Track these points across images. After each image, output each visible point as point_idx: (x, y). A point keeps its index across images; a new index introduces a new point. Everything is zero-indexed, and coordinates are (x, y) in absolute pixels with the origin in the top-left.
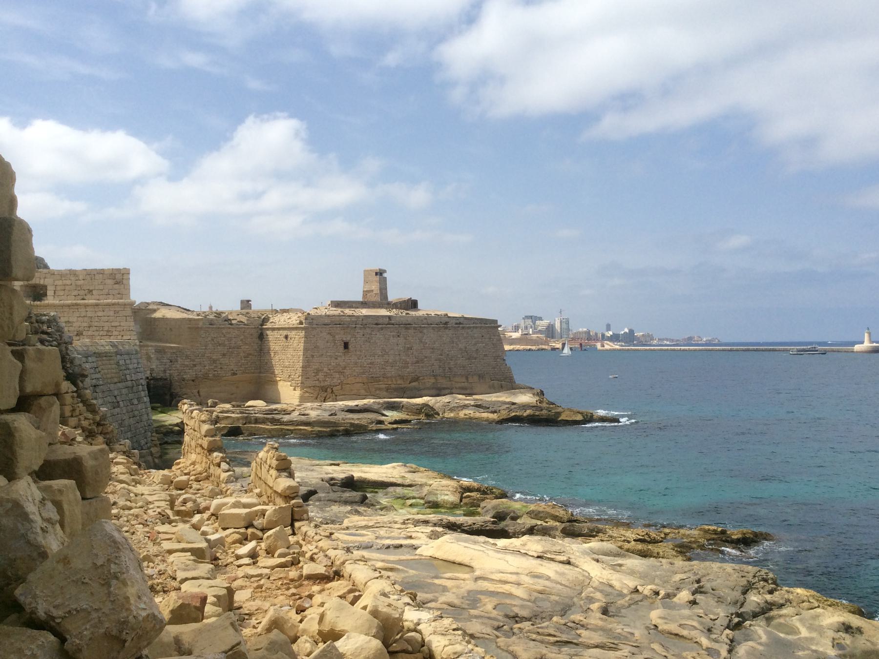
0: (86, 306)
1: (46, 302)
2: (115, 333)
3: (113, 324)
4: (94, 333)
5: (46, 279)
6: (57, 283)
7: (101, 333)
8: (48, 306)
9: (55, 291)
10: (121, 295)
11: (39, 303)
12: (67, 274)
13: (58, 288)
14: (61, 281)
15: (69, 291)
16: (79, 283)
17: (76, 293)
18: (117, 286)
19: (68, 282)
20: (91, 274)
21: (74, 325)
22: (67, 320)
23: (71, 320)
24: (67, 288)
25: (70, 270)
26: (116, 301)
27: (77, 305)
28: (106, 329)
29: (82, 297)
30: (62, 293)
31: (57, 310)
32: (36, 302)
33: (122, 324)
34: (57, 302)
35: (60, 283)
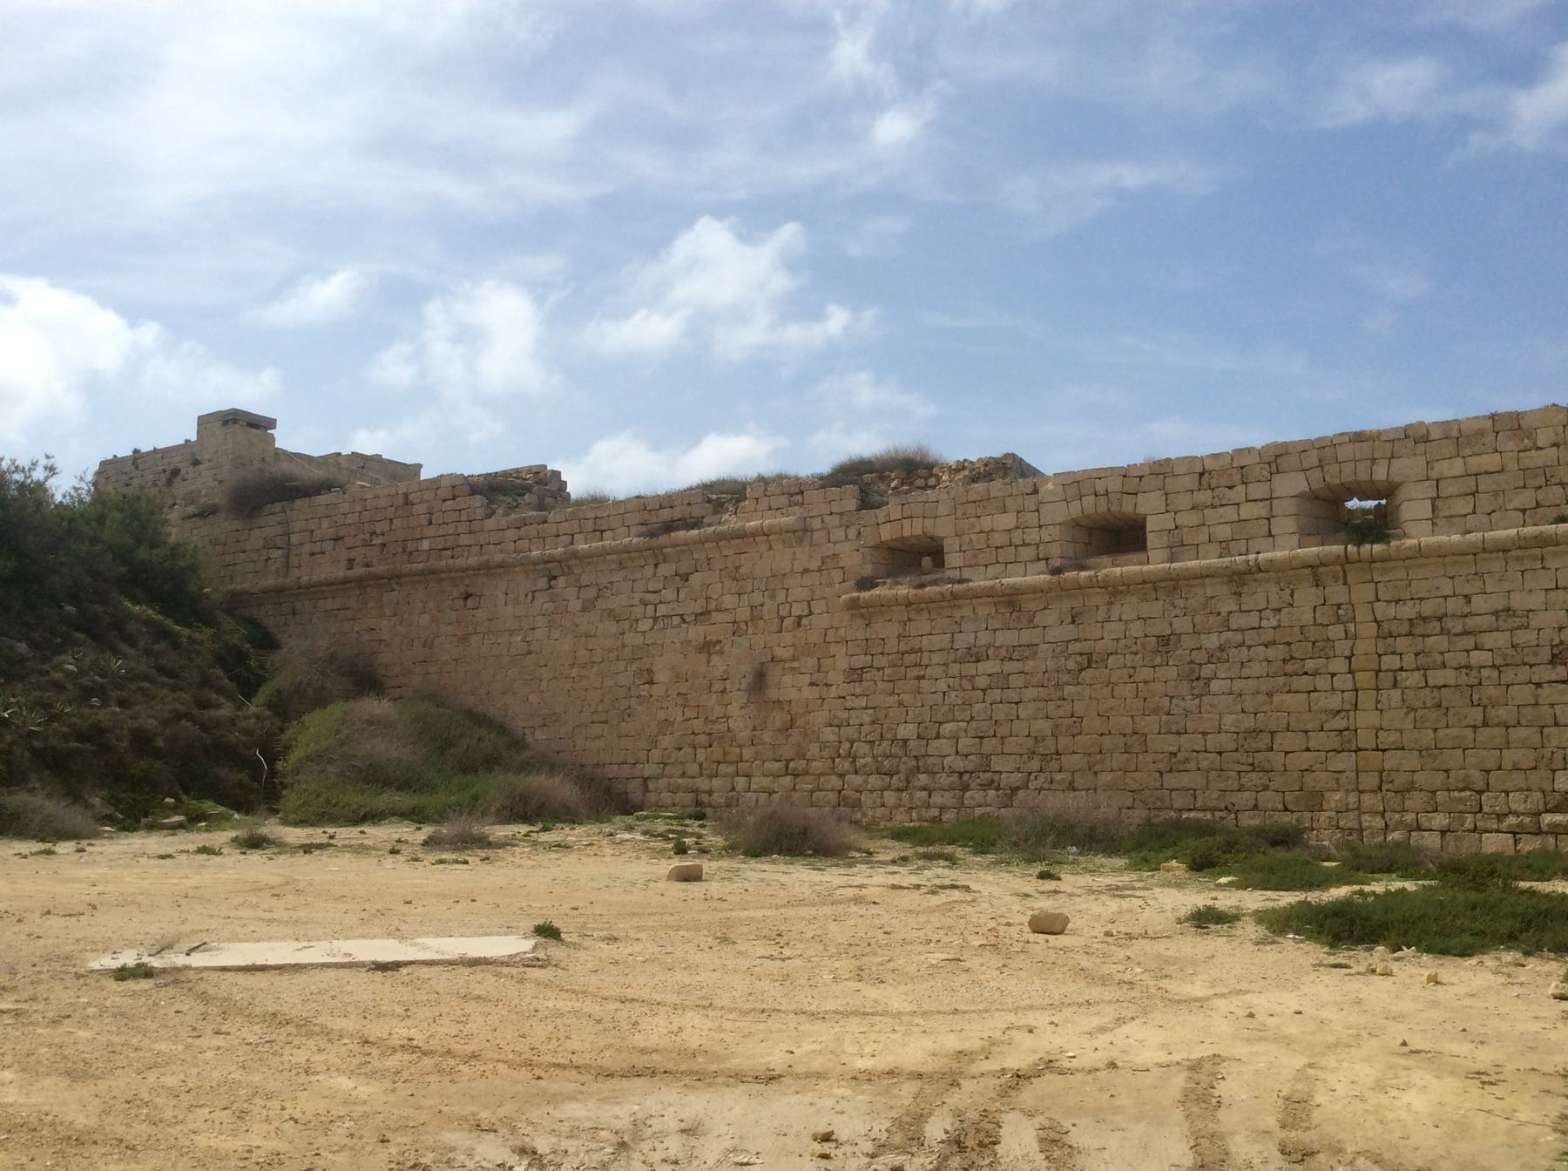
1: (1409, 542)
5: (1395, 462)
6: (1443, 468)
8: (1419, 553)
9: (1433, 500)
11: (1377, 548)
12: (1481, 433)
13: (1449, 489)
14: (1459, 461)
15: (1496, 493)
16: (1535, 459)
17: (1525, 498)
19: (1490, 461)
22: (1500, 603)
23: (1517, 601)
24: (1485, 483)
25: (1493, 417)
27: (1542, 541)
29: (1555, 512)
30: (1463, 506)
31: (1452, 571)
34: (1456, 538)
35: (1457, 467)
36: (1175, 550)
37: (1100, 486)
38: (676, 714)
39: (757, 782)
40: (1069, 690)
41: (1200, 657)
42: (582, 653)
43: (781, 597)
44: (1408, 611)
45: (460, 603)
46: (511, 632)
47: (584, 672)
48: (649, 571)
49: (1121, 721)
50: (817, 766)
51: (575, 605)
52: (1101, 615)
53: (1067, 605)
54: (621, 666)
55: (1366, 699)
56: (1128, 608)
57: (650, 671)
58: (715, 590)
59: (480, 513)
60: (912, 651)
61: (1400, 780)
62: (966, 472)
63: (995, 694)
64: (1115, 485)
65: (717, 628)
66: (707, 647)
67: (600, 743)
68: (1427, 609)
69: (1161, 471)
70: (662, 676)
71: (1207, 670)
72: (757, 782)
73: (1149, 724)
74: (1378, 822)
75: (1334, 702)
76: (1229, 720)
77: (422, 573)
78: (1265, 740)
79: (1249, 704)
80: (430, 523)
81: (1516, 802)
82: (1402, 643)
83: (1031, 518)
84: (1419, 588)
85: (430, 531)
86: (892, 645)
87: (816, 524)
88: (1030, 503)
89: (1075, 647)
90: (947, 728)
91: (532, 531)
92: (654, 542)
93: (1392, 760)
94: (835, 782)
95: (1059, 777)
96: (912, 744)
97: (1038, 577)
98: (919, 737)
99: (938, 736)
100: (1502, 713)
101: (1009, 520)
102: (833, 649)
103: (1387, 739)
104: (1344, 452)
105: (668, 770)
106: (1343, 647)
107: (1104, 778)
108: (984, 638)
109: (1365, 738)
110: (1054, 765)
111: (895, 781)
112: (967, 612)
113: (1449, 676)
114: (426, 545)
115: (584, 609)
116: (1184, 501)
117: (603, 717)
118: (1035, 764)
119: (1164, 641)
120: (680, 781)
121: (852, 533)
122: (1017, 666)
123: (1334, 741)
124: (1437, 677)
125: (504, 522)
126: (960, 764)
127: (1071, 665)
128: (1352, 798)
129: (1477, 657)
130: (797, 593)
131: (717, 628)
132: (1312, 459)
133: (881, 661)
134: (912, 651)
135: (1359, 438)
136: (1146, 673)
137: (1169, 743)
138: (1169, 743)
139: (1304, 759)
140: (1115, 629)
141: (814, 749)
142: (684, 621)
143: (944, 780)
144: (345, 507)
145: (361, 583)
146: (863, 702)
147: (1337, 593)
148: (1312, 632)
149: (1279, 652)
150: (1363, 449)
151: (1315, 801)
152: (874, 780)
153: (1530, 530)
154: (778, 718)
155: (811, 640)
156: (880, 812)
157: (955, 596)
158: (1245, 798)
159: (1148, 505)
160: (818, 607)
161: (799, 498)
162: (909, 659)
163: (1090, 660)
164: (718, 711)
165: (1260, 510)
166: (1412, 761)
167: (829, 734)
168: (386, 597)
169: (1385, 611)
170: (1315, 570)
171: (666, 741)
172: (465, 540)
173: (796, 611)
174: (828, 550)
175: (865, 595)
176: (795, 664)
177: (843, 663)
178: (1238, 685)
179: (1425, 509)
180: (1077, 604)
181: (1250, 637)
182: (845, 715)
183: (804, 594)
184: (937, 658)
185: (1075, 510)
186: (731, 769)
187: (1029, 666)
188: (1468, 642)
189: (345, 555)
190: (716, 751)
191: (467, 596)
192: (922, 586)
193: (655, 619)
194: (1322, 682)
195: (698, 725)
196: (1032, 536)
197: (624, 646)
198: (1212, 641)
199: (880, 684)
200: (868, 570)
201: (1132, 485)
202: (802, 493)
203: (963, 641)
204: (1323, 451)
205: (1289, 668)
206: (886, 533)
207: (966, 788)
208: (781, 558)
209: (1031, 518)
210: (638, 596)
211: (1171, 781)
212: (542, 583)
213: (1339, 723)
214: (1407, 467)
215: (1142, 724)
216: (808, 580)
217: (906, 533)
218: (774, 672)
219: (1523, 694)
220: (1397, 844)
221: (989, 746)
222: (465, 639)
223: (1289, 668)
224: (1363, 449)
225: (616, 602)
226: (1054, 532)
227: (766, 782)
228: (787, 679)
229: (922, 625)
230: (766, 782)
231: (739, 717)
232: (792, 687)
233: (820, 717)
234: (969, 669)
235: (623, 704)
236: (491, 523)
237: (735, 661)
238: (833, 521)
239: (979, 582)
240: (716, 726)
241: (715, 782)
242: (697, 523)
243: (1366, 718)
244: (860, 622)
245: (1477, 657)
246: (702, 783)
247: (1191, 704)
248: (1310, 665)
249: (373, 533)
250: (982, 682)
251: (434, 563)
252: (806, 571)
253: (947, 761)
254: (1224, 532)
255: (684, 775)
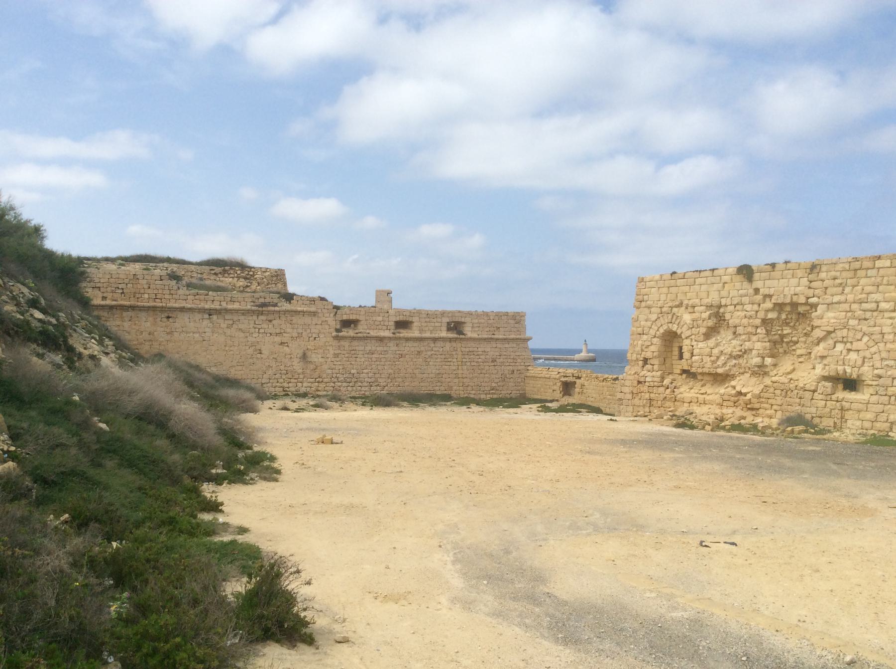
0: (497, 339)
2: (519, 360)
3: (518, 354)
4: (504, 360)
7: (509, 360)
10: (519, 331)
11: (463, 336)
16: (490, 322)
17: (487, 329)
18: (517, 325)
19: (483, 321)
20: (499, 315)
21: (489, 354)
24: (481, 325)
26: (518, 337)
28: (512, 357)
32: (461, 336)
33: (524, 354)
35: (476, 321)
36: (421, 331)
37: (404, 314)
38: (273, 364)
39: (305, 385)
40: (397, 363)
41: (427, 357)
42: (229, 342)
43: (309, 331)
44: (467, 350)
45: (165, 320)
46: (194, 333)
47: (231, 349)
48: (255, 317)
49: (410, 370)
50: (325, 380)
51: (224, 326)
52: (404, 345)
53: (396, 342)
54: (247, 348)
55: (460, 367)
56: (410, 344)
57: (260, 350)
58: (283, 326)
59: (175, 288)
60: (353, 350)
61: (467, 384)
62: (267, 274)
63: (378, 363)
64: (408, 314)
65: (286, 338)
66: (282, 343)
67: (242, 372)
68: (471, 349)
69: (419, 312)
70: (266, 352)
71: (428, 360)
72: (305, 385)
73: (417, 371)
74: (463, 392)
75: (454, 368)
76: (434, 371)
77: (149, 307)
78: (440, 376)
79: (437, 367)
80: (149, 288)
81: (486, 388)
82: (466, 356)
83: (386, 319)
84: (469, 345)
85: (149, 291)
86: (347, 348)
87: (319, 311)
88: (386, 315)
89: (398, 352)
90: (365, 371)
91: (202, 297)
92: (260, 309)
93: (465, 380)
94: (332, 384)
95: (396, 384)
96: (355, 375)
97: (387, 334)
98: (358, 373)
99: (363, 373)
100: (484, 371)
101: (380, 319)
102: (328, 348)
103: (464, 376)
104: (456, 315)
105: (271, 381)
106: (456, 356)
107: (407, 384)
108: (374, 348)
109: (460, 376)
110: (394, 381)
111: (351, 384)
112: (369, 341)
113: (475, 364)
114: (146, 296)
115: (227, 328)
116: (423, 320)
117: (242, 364)
118: (390, 381)
119: (419, 352)
120: (277, 384)
121: (332, 315)
122: (383, 356)
123: (454, 376)
124: (473, 364)
125: (188, 292)
126: (370, 380)
127: (397, 357)
128: (458, 388)
129: (479, 360)
130: (313, 331)
131: (286, 338)
132: (450, 315)
133: (345, 352)
134: (353, 350)
135: (459, 312)
136: (415, 360)
137: (421, 376)
138: (421, 376)
139: (449, 380)
140: (407, 349)
141: (324, 376)
142: (271, 335)
143: (365, 384)
144: (101, 276)
145: (111, 308)
146: (339, 363)
147: (454, 344)
148: (450, 353)
149: (443, 357)
150: (459, 314)
151: (451, 388)
152: (344, 384)
153: (490, 336)
154: (312, 367)
155: (320, 345)
156: (347, 392)
157: (367, 337)
158: (437, 388)
159: (415, 319)
160: (322, 336)
161: (313, 302)
162: (353, 352)
163: (401, 356)
164: (289, 364)
165: (439, 324)
166: (468, 380)
167: (330, 371)
168: (125, 314)
169: (463, 349)
170: (450, 340)
171: (270, 372)
172: (167, 297)
173: (314, 336)
174: (324, 319)
175: (340, 334)
176: (316, 351)
177: (332, 352)
178: (435, 363)
179: (470, 329)
180: (398, 342)
181: (437, 353)
182: (334, 366)
183: (317, 331)
184: (361, 352)
185: (398, 319)
186: (296, 381)
187: (386, 356)
188: (478, 357)
189: (100, 295)
190: (289, 376)
191: (168, 317)
192: (357, 333)
193: (259, 333)
194: (452, 364)
195: (282, 367)
196: (386, 323)
197: (248, 341)
198: (429, 353)
199: (345, 359)
200: (338, 327)
201: (412, 315)
202: (314, 301)
203: (368, 348)
204: (453, 313)
205: (446, 360)
206: (345, 317)
207: (371, 386)
208: (307, 320)
209: (386, 319)
210: (251, 326)
211: (422, 384)
212: (207, 316)
213: (455, 372)
214: (468, 320)
215: (415, 371)
216: (318, 327)
217: (351, 318)
218: (309, 353)
219: (487, 368)
220: (466, 397)
221: (377, 376)
222: (170, 333)
223: (446, 360)
224: (459, 314)
225: (241, 326)
226: (393, 323)
227: (309, 384)
228: (313, 355)
229: (355, 343)
230: (309, 384)
231: (297, 366)
232: (315, 358)
233: (325, 367)
234: (370, 356)
235: (251, 361)
236: (181, 292)
237: (296, 349)
238: (326, 311)
239: (373, 333)
240: (289, 368)
241: (290, 385)
242: (276, 305)
243: (460, 372)
244: (337, 341)
245: (479, 360)
246: (285, 385)
247: (425, 367)
248: (449, 360)
249: (118, 288)
250: (374, 360)
251: (151, 304)
252: (316, 324)
253: (366, 379)
254: (431, 328)
255: (278, 382)
